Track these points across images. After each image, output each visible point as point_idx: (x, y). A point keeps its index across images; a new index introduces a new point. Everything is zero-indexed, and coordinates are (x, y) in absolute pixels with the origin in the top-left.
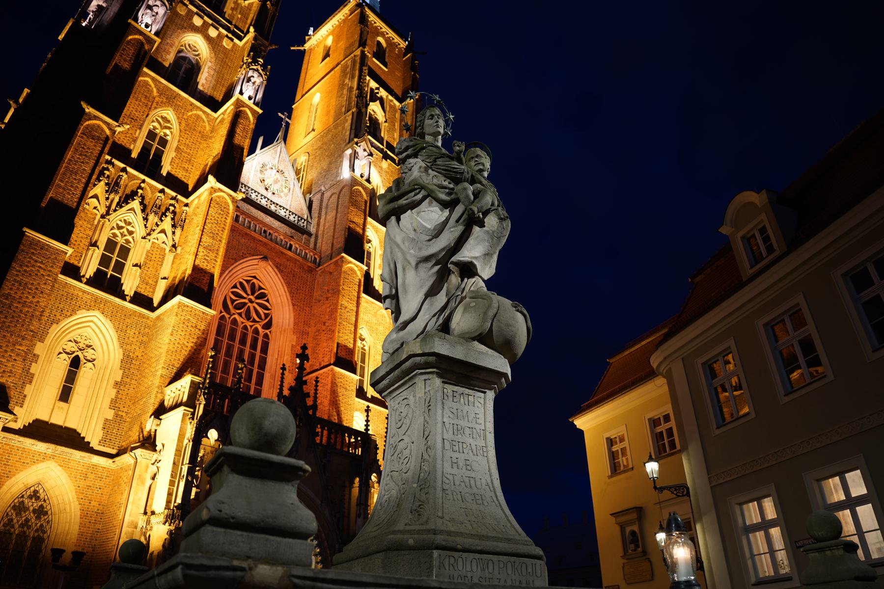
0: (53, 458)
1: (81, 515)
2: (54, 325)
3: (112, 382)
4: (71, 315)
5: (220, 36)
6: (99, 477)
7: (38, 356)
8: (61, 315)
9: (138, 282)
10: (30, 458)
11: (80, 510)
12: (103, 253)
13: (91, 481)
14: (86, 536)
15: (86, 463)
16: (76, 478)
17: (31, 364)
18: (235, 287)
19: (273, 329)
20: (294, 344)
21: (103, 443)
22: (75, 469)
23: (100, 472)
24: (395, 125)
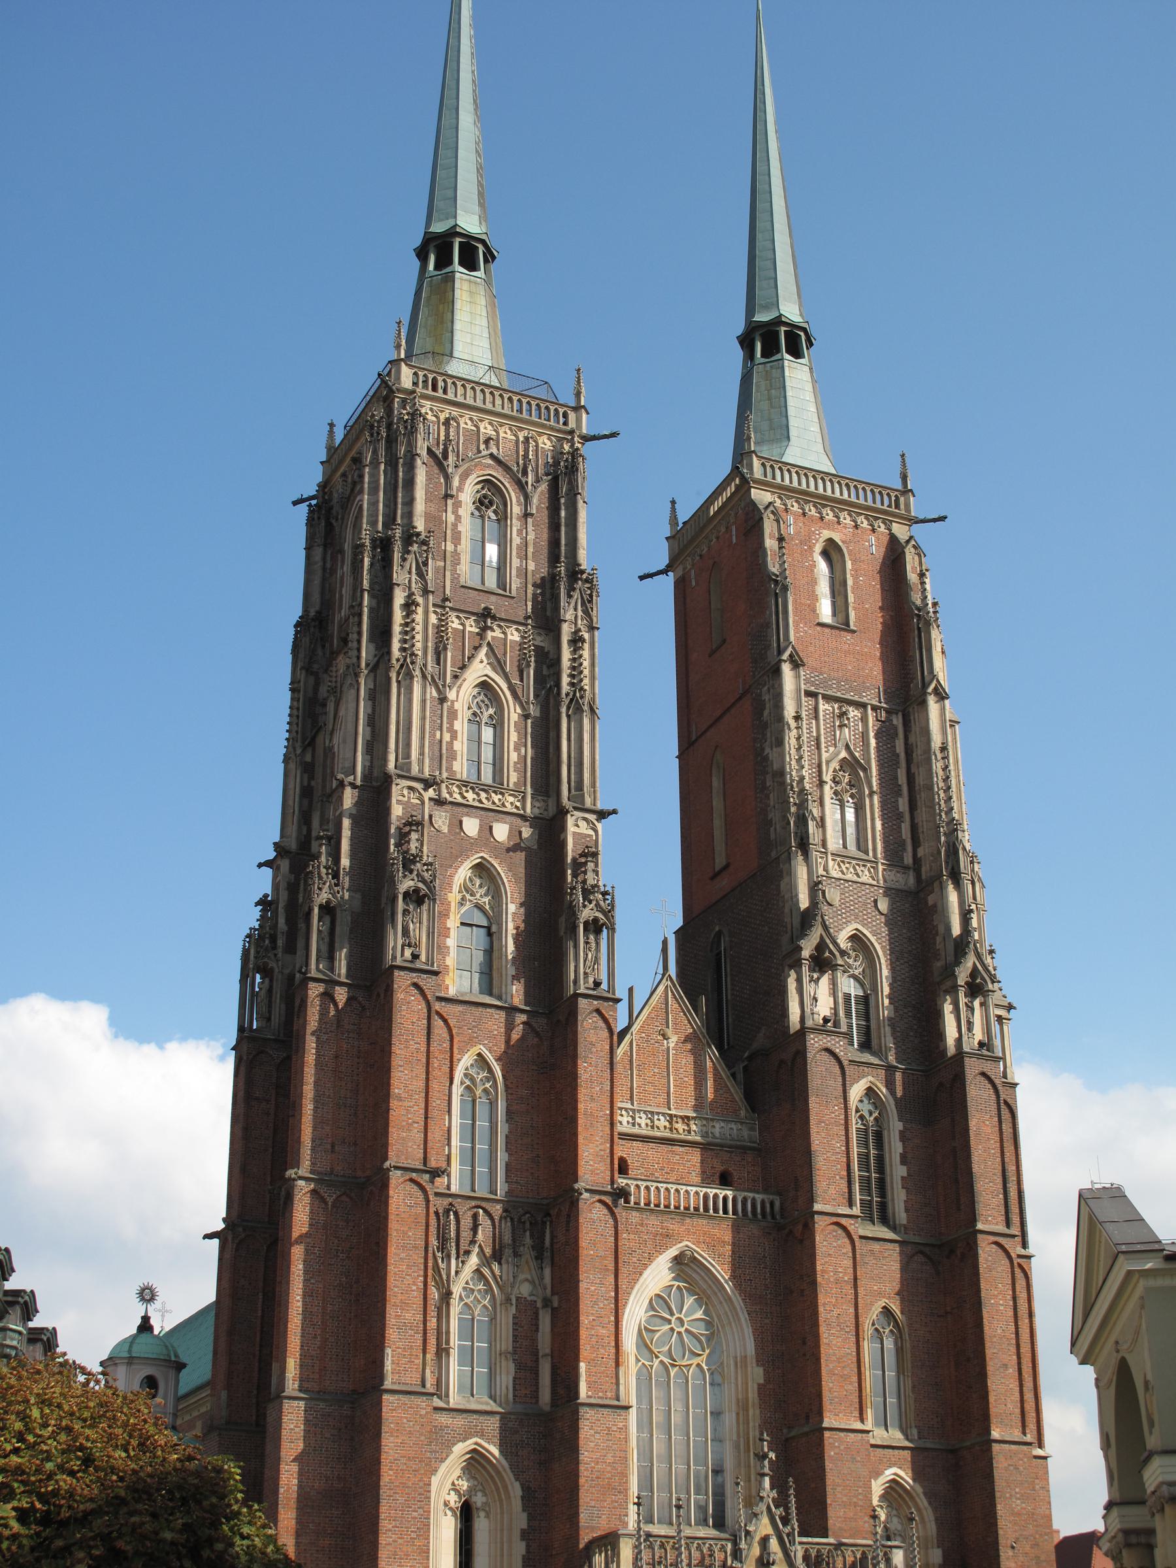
3: (517, 1535)
4: (447, 1456)
5: (516, 832)
18: (651, 1306)
20: (762, 1381)
24: (896, 778)
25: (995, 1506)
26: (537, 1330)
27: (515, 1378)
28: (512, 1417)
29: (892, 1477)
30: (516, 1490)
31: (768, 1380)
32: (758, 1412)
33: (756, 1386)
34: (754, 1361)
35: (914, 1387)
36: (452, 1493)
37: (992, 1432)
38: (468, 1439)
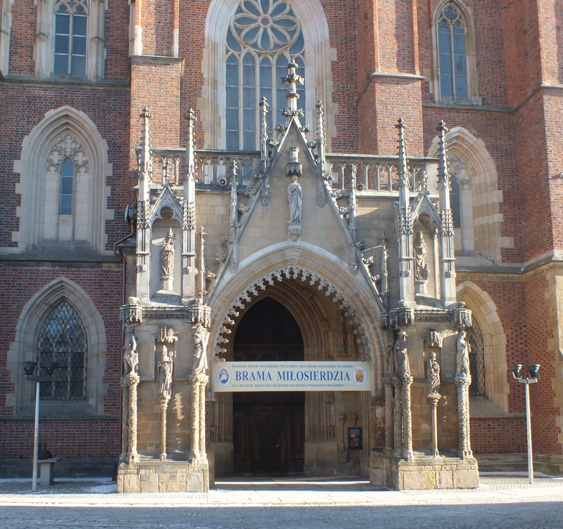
0: (63, 274)
1: (105, 324)
2: (26, 138)
4: (40, 120)
6: (114, 283)
7: (19, 175)
8: (29, 124)
9: (105, 54)
10: (40, 279)
11: (103, 319)
12: (56, 36)
13: (108, 288)
14: (116, 344)
15: (97, 272)
16: (91, 288)
17: (15, 185)
18: (239, 10)
19: (308, 47)
20: (335, 59)
21: (110, 247)
22: (87, 280)
23: (115, 278)
25: (544, 143)
26: (129, 21)
27: (106, 61)
28: (101, 88)
29: (457, 134)
30: (103, 146)
31: (341, 57)
32: (332, 82)
33: (329, 64)
34: (329, 43)
35: (478, 65)
36: (56, 154)
37: (543, 82)
38: (59, 106)
